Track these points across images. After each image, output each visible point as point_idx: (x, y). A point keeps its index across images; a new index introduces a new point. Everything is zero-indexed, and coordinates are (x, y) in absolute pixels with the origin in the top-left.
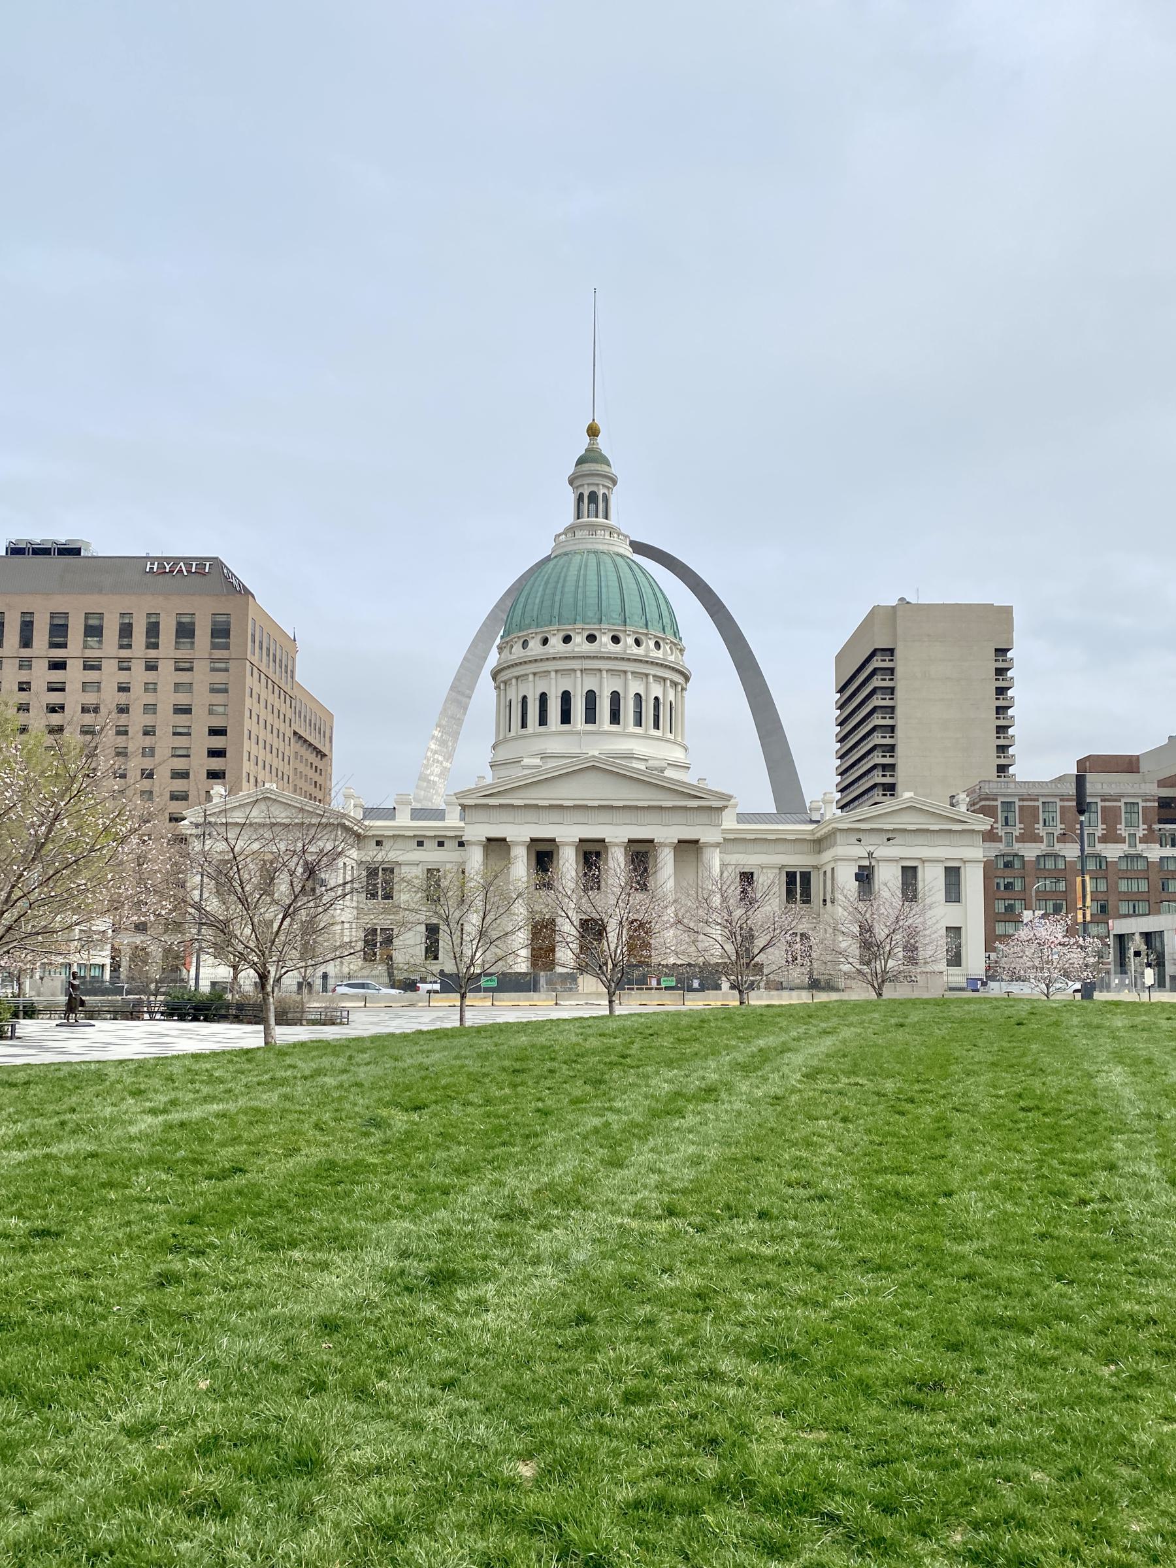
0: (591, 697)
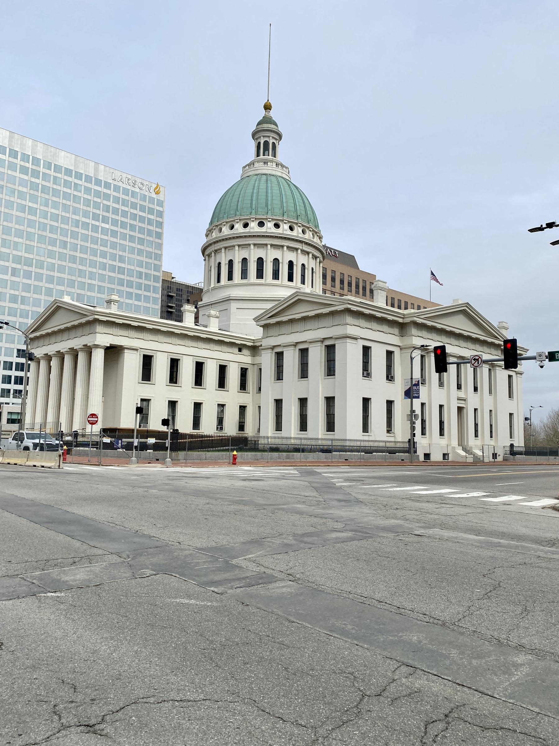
0: (260, 262)
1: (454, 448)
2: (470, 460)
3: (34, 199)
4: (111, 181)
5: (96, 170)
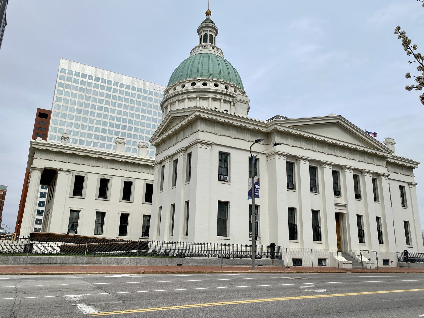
1: (331, 253)
2: (349, 265)
3: (107, 103)
4: (153, 91)
5: (144, 85)
